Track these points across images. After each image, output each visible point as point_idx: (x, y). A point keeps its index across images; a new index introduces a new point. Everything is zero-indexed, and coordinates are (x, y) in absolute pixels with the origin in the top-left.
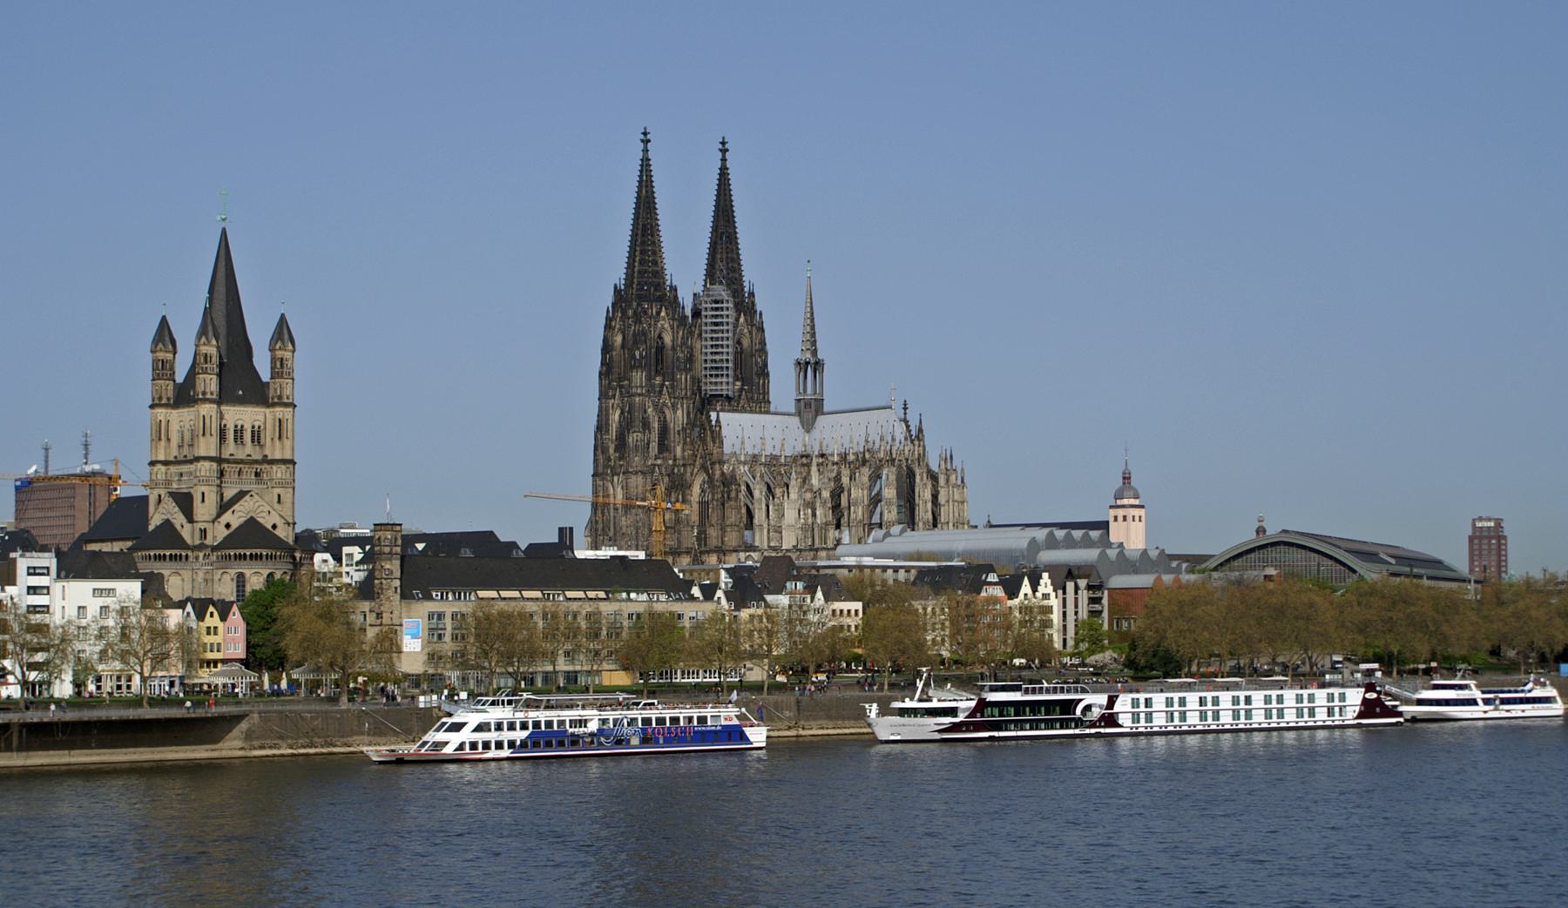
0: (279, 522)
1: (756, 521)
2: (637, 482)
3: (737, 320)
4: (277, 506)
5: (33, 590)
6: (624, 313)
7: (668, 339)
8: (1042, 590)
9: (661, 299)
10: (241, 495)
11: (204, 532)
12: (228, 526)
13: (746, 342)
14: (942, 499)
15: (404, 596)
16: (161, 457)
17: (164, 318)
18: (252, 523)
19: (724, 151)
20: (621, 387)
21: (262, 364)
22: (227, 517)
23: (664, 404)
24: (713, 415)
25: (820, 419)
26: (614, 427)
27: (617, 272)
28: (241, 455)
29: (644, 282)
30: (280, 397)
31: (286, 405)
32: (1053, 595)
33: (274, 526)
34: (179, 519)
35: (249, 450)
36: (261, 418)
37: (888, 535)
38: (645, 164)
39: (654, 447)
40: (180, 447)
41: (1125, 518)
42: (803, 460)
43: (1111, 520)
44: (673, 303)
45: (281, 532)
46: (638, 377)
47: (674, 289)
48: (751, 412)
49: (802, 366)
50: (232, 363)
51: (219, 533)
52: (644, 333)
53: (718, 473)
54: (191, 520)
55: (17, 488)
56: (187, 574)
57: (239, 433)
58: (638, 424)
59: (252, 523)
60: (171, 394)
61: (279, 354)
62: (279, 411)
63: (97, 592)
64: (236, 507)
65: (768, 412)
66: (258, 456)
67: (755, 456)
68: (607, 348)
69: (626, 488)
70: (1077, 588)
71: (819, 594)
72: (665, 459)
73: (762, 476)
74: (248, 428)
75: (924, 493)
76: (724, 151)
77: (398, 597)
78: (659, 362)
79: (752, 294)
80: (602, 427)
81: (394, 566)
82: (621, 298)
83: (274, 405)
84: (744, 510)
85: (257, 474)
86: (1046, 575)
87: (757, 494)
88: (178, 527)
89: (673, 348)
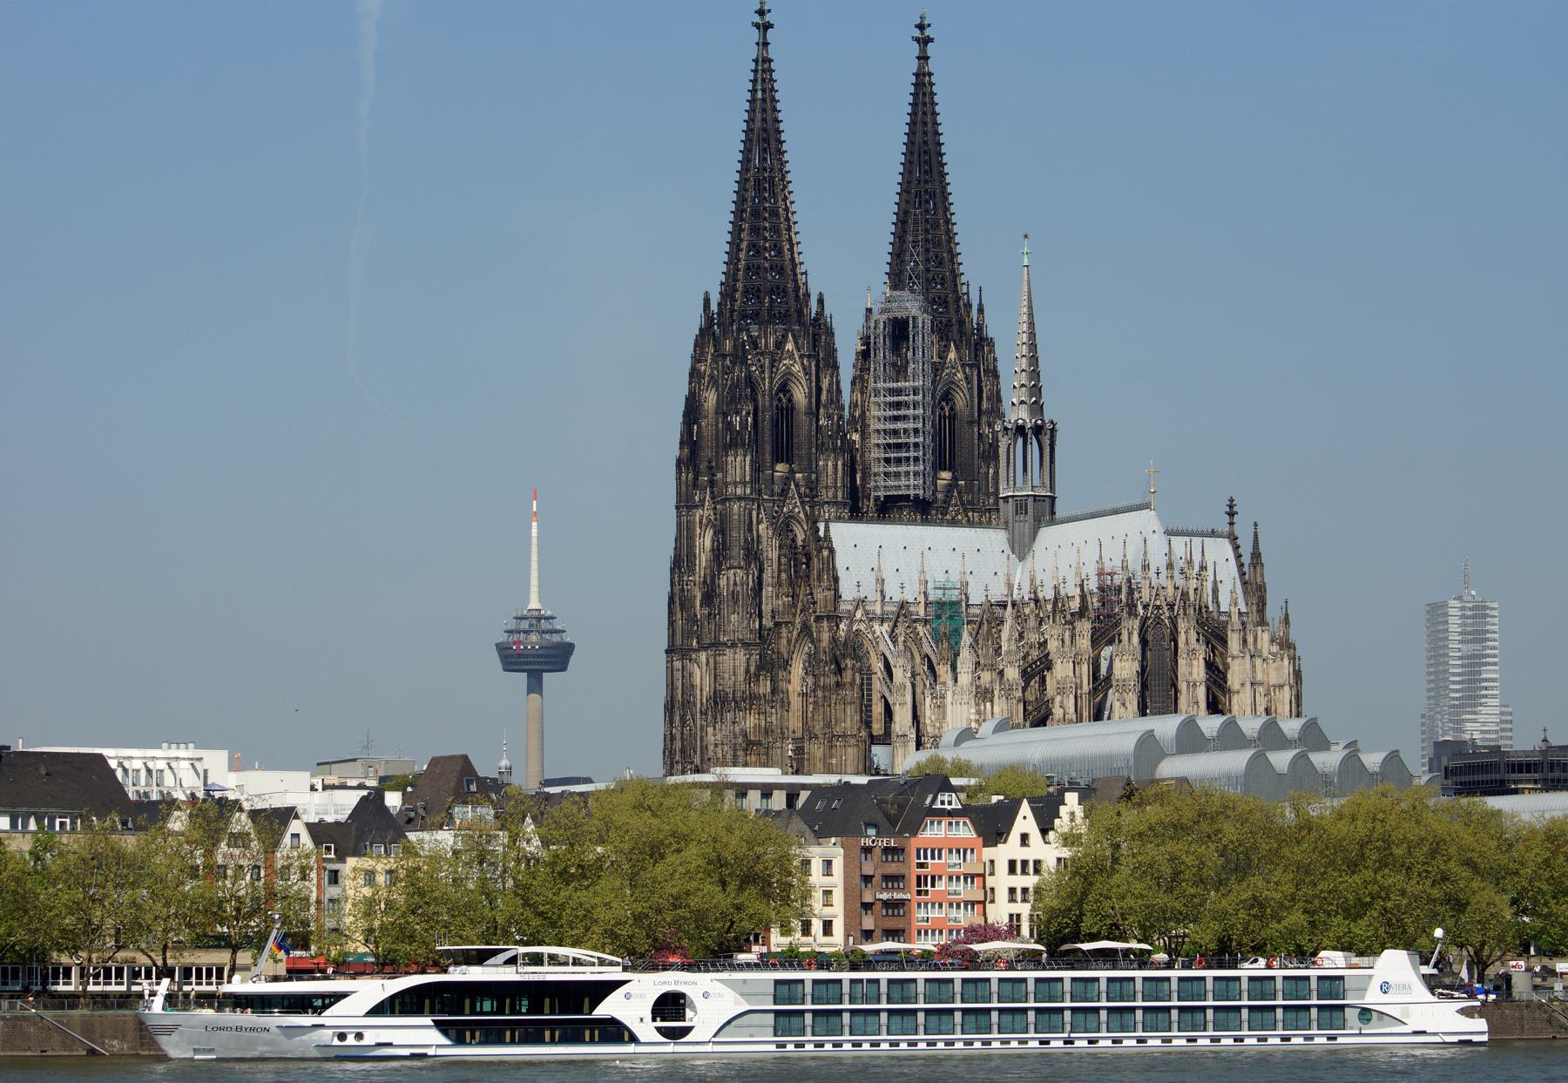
3: (942, 356)
7: (800, 395)
13: (960, 400)
14: (1234, 679)
19: (924, 42)
23: (791, 517)
24: (822, 526)
25: (1048, 535)
26: (703, 559)
27: (709, 274)
29: (761, 287)
38: (763, 71)
42: (992, 615)
48: (970, 524)
52: (751, 382)
53: (826, 636)
58: (737, 553)
67: (903, 605)
75: (1192, 670)
76: (924, 42)
78: (780, 437)
80: (682, 561)
86: (1072, 798)
87: (898, 674)
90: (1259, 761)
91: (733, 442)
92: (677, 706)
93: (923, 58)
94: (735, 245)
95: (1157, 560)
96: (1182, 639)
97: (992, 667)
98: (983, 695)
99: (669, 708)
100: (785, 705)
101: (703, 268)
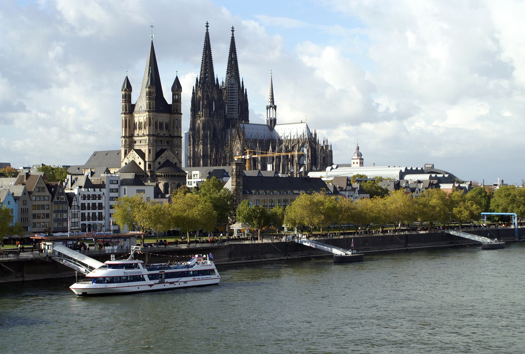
5: (112, 190)
10: (162, 151)
12: (159, 163)
22: (159, 159)
24: (241, 125)
30: (177, 110)
34: (138, 160)
35: (165, 132)
36: (168, 119)
37: (332, 169)
47: (217, 79)
63: (139, 191)
64: (162, 155)
66: (167, 135)
83: (175, 113)
85: (167, 142)
88: (138, 164)
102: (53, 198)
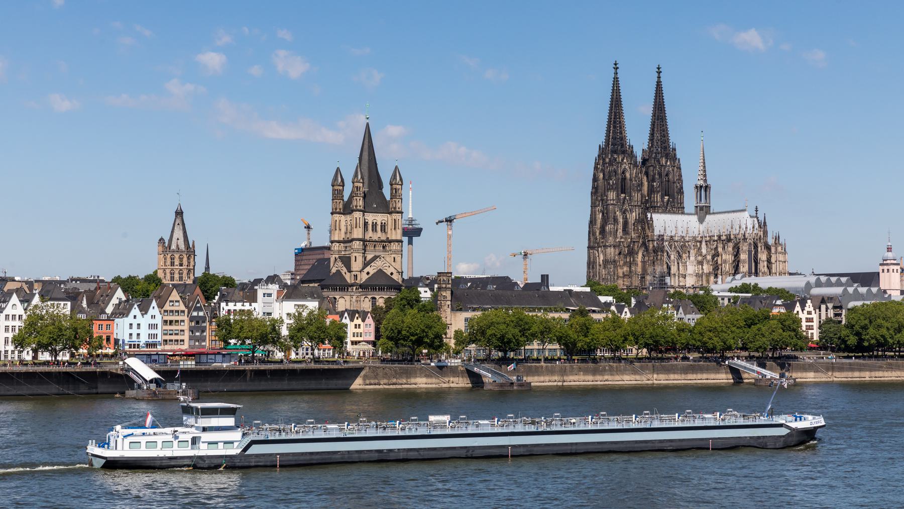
0: (394, 272)
1: (672, 272)
2: (611, 252)
4: (393, 264)
6: (604, 160)
7: (628, 175)
8: (807, 309)
9: (624, 152)
11: (356, 276)
12: (368, 273)
14: (773, 260)
15: (452, 310)
16: (336, 239)
17: (338, 170)
18: (380, 272)
19: (659, 73)
20: (602, 200)
21: (387, 192)
22: (368, 269)
23: (626, 210)
27: (601, 139)
28: (375, 238)
29: (615, 142)
31: (398, 212)
32: (813, 312)
33: (392, 274)
34: (344, 270)
35: (379, 235)
38: (616, 81)
39: (620, 231)
40: (346, 233)
41: (888, 270)
42: (697, 241)
43: (881, 271)
44: (632, 155)
45: (395, 277)
46: (612, 195)
47: (631, 147)
49: (699, 188)
50: (370, 189)
51: (363, 277)
53: (651, 246)
54: (350, 271)
55: (296, 255)
56: (347, 298)
57: (374, 226)
58: (611, 220)
59: (380, 272)
60: (341, 206)
61: (394, 186)
62: (395, 216)
65: (683, 213)
66: (384, 238)
67: (671, 237)
68: (595, 179)
69: (605, 255)
70: (827, 309)
71: (681, 310)
72: (626, 239)
73: (675, 247)
74: (379, 223)
75: (763, 256)
76: (659, 73)
77: (449, 310)
78: (623, 187)
79: (674, 150)
80: (592, 222)
81: (448, 294)
82: (603, 152)
84: (665, 266)
85: (384, 247)
86: (809, 301)
87: (672, 257)
89: (631, 180)
90: (845, 290)
91: (609, 188)
92: (591, 264)
93: (659, 77)
94: (608, 131)
95: (750, 226)
96: (759, 249)
97: (701, 255)
98: (700, 263)
99: (589, 264)
100: (637, 265)
101: (599, 137)
102: (189, 313)
